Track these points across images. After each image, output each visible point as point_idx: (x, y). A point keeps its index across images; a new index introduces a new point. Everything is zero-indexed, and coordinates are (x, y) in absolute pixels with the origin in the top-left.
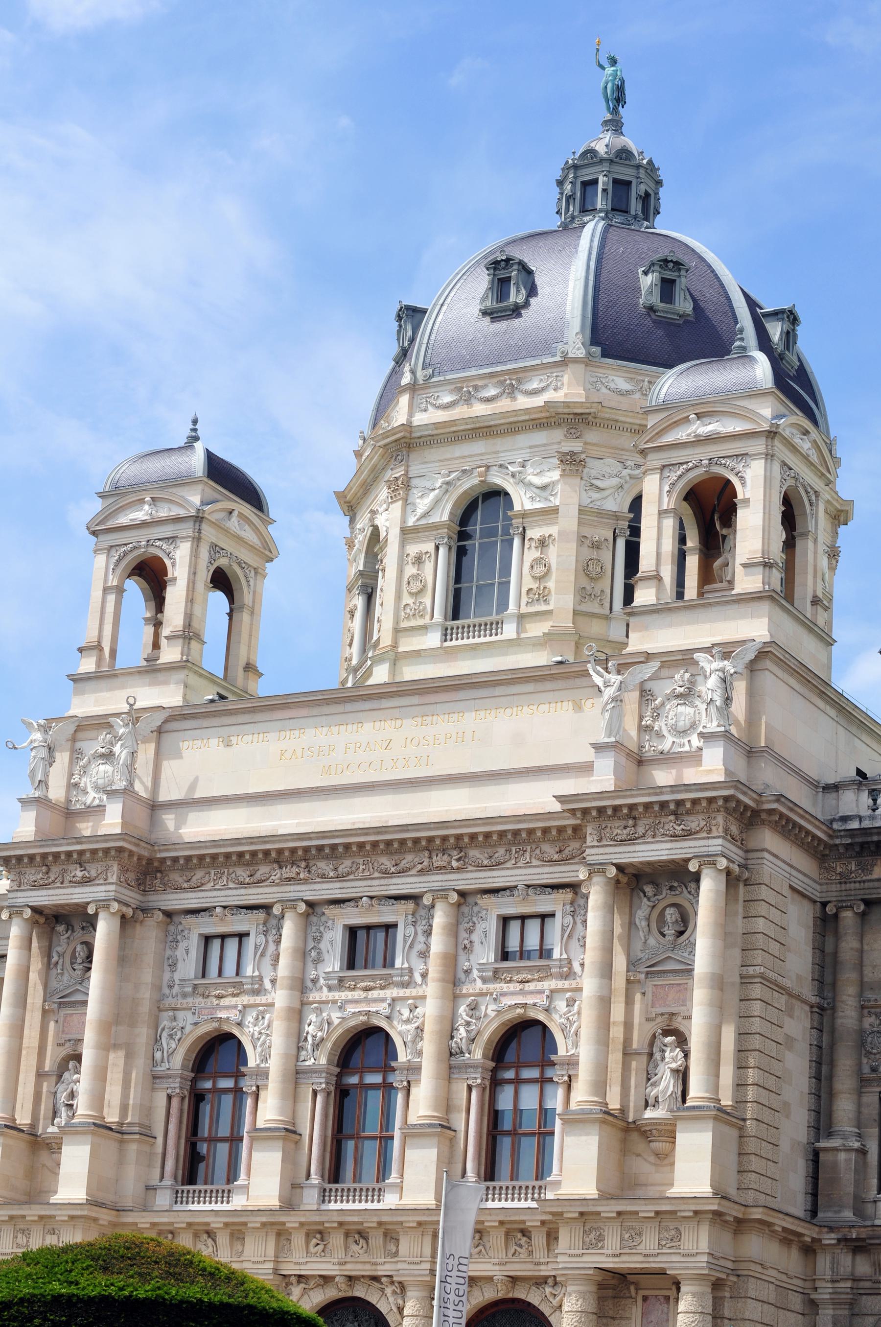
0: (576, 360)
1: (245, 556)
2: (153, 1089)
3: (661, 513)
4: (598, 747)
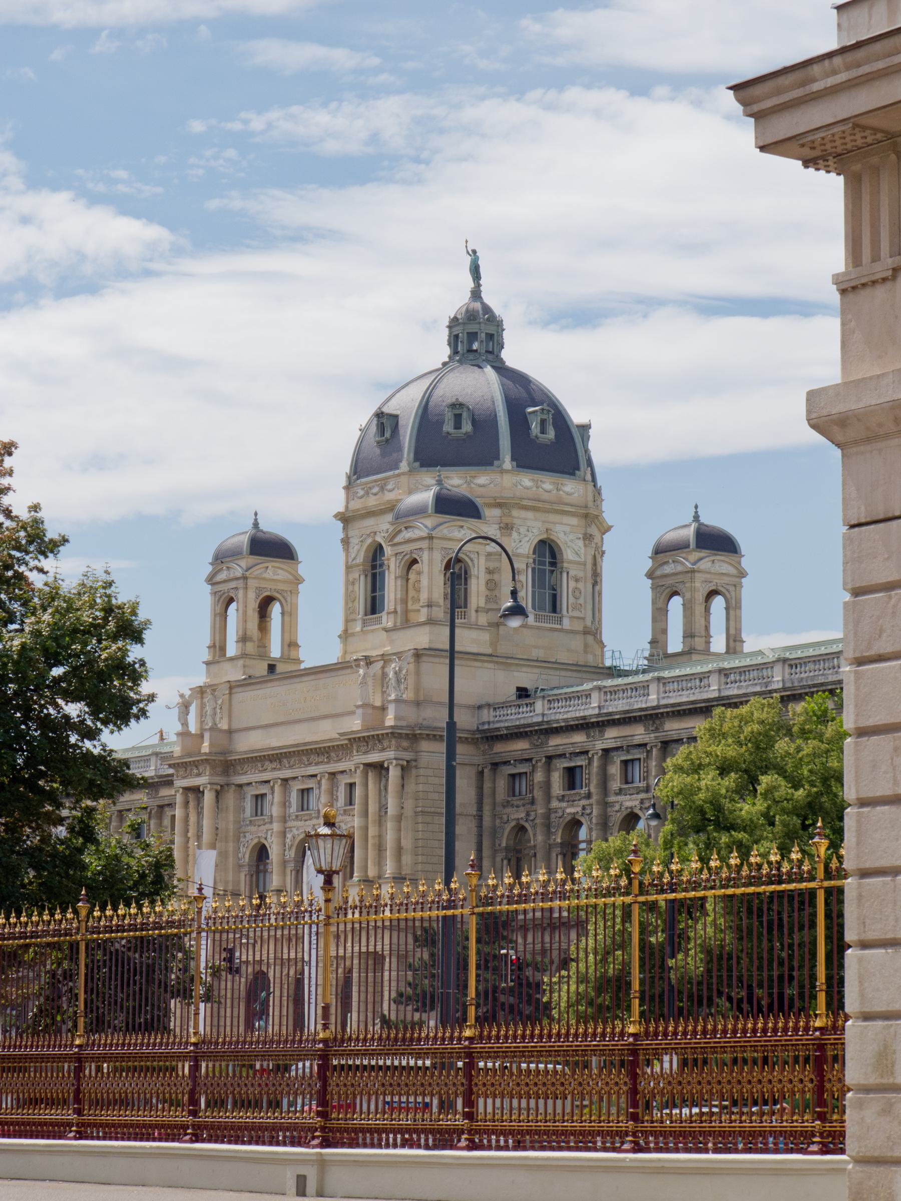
0: (403, 474)
1: (281, 587)
2: (240, 872)
3: (396, 578)
4: (358, 707)
